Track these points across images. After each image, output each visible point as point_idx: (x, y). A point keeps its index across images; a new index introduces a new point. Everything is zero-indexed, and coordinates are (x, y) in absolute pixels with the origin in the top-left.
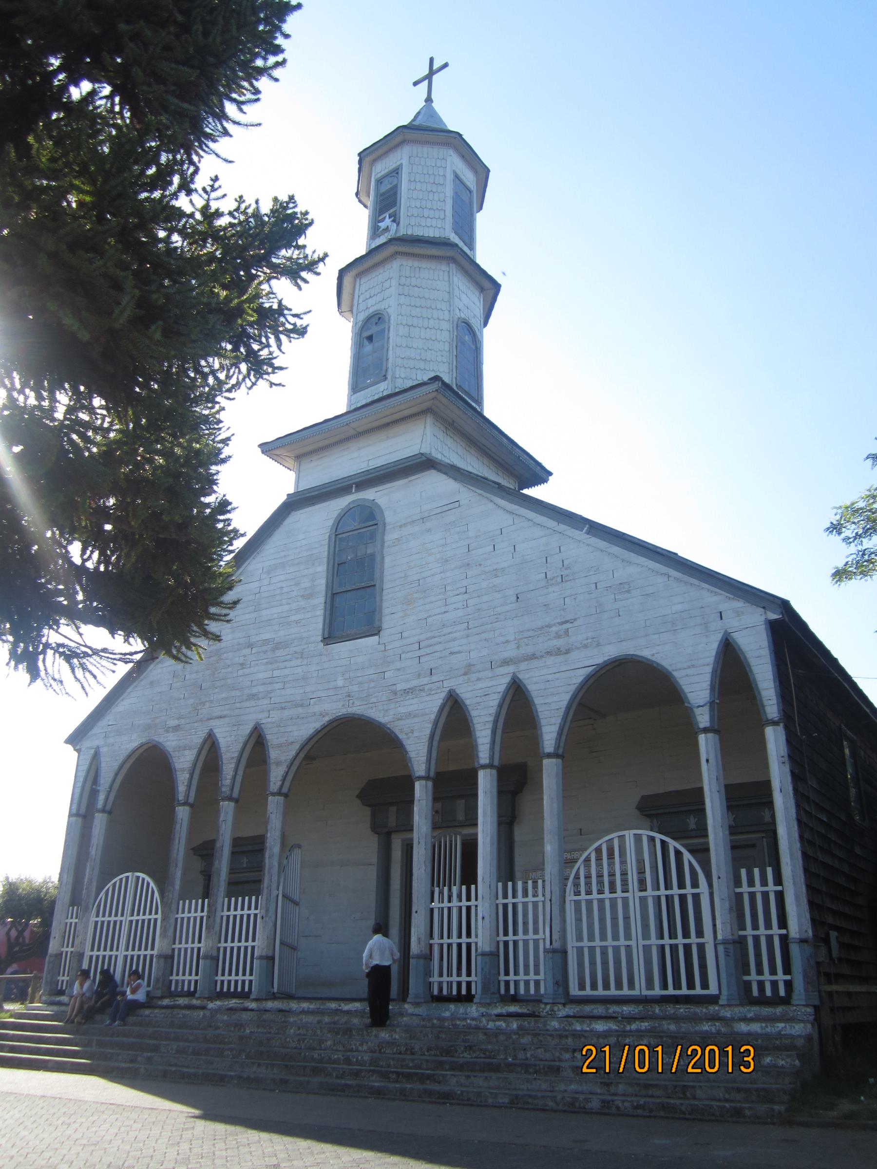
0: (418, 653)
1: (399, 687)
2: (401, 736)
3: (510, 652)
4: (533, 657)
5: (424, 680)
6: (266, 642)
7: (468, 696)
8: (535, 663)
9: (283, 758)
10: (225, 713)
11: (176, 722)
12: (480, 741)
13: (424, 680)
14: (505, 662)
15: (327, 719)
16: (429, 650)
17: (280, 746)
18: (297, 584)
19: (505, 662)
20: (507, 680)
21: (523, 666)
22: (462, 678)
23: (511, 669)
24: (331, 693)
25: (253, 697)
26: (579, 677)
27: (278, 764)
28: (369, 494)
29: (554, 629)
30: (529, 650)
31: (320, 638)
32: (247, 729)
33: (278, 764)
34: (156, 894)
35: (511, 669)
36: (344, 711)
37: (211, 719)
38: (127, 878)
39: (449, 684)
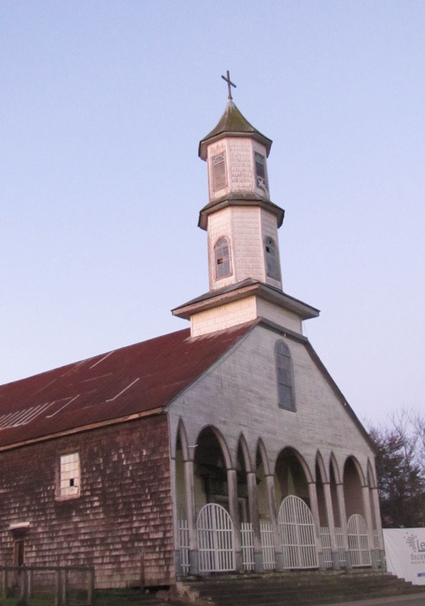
1: (304, 440)
6: (257, 393)
7: (322, 452)
10: (245, 424)
11: (223, 419)
14: (330, 444)
17: (270, 452)
19: (330, 444)
22: (320, 445)
25: (256, 420)
31: (277, 403)
32: (256, 438)
33: (271, 460)
34: (229, 517)
35: (330, 447)
37: (240, 425)
38: (211, 506)
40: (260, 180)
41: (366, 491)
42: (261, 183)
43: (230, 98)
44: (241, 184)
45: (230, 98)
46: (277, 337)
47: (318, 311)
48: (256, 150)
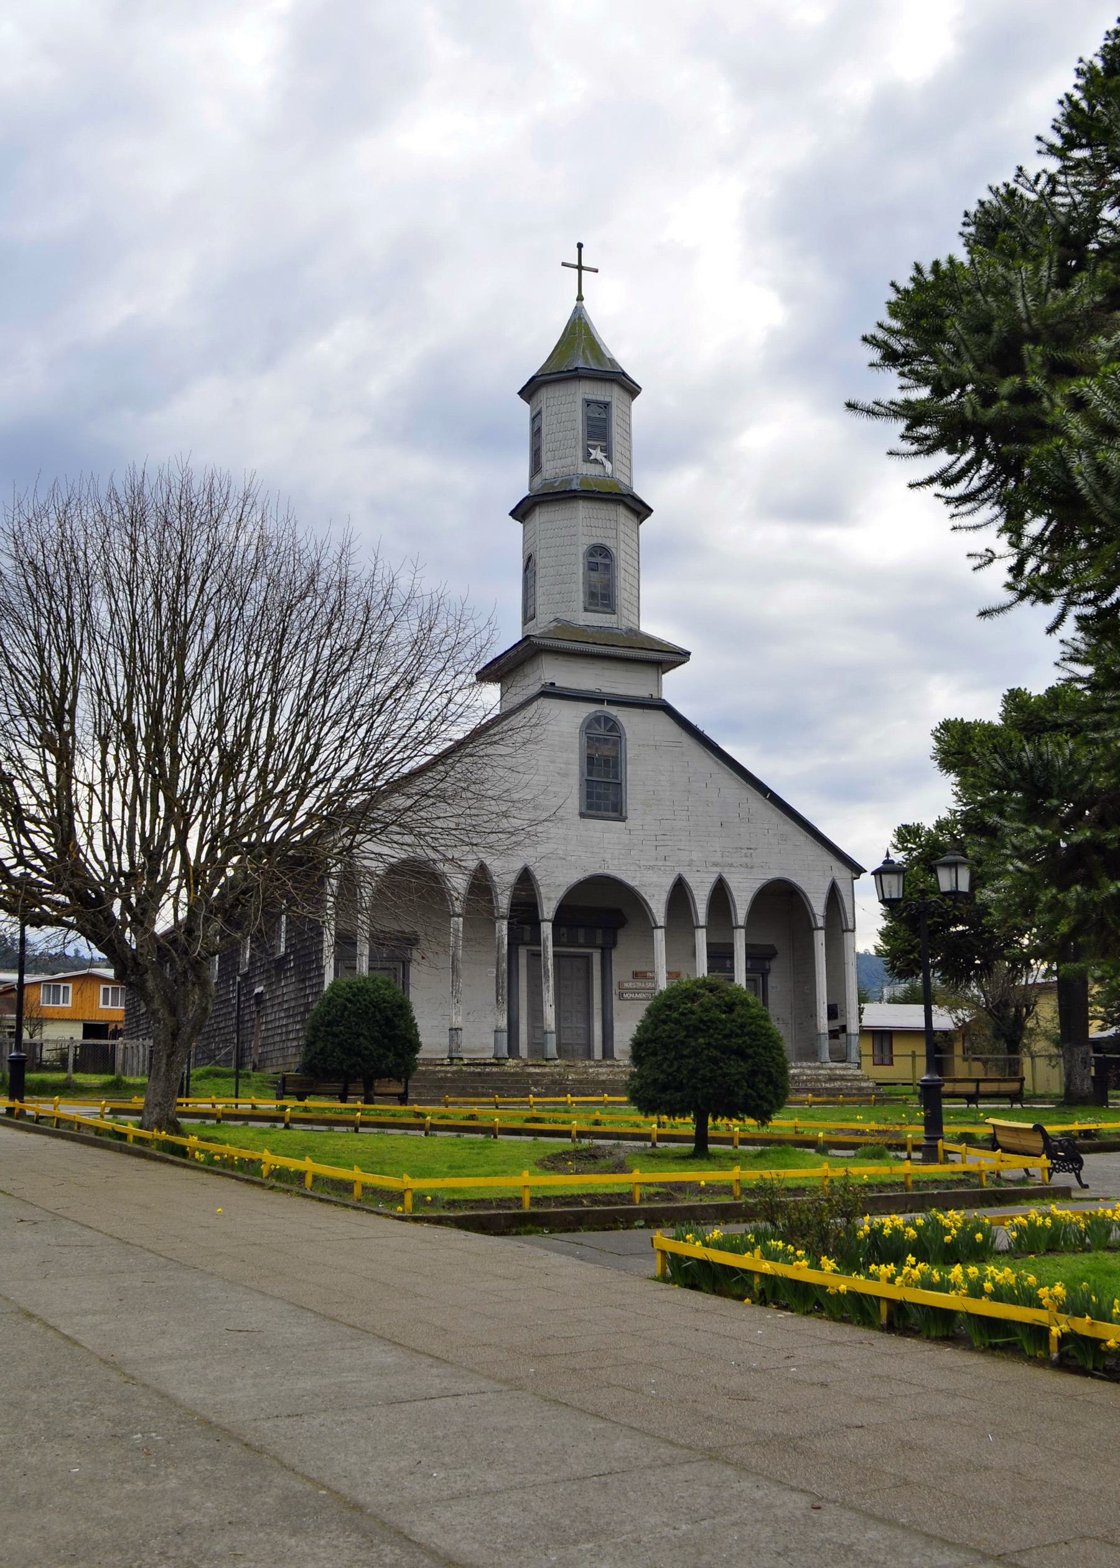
0: (656, 843)
1: (642, 863)
2: (646, 898)
3: (717, 858)
4: (731, 865)
5: (660, 863)
7: (691, 880)
8: (733, 869)
9: (553, 895)
12: (699, 911)
13: (660, 863)
14: (715, 865)
15: (587, 874)
16: (662, 843)
17: (549, 885)
18: (553, 762)
19: (715, 865)
20: (716, 876)
21: (726, 869)
23: (719, 869)
24: (589, 855)
26: (758, 885)
27: (549, 899)
28: (613, 711)
29: (744, 851)
30: (729, 860)
31: (577, 812)
33: (549, 899)
35: (719, 869)
36: (600, 871)
39: (679, 870)
40: (594, 447)
41: (820, 937)
42: (597, 454)
43: (580, 298)
44: (559, 463)
45: (580, 298)
46: (588, 710)
47: (689, 653)
48: (586, 397)
